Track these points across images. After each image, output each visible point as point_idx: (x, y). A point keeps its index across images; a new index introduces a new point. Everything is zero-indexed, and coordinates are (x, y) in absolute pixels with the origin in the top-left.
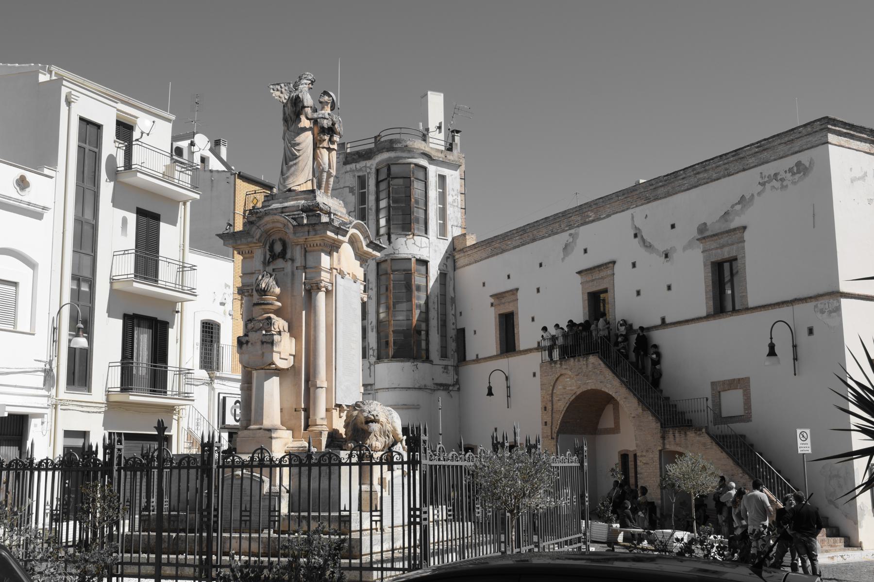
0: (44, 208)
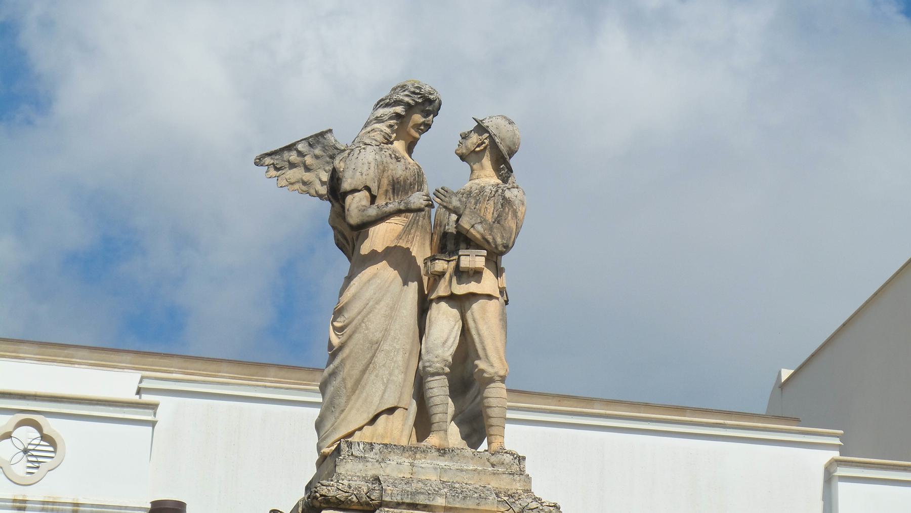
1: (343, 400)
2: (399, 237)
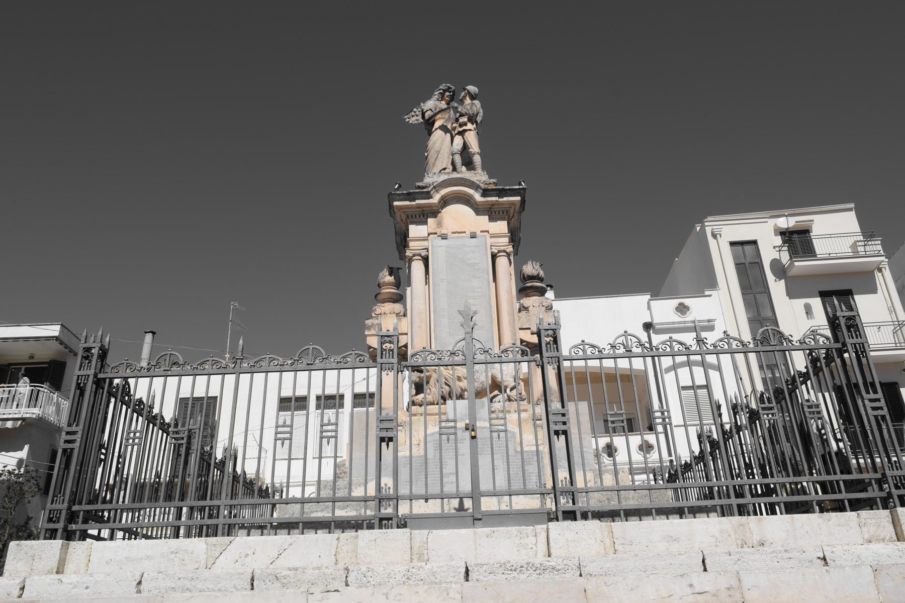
0: (709, 321)
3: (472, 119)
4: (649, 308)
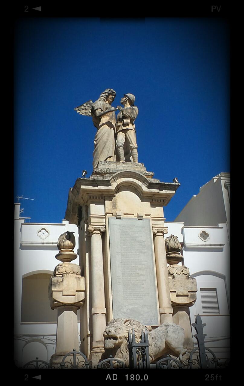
1: (99, 156)
2: (109, 120)
3: (131, 122)
4: (182, 232)
